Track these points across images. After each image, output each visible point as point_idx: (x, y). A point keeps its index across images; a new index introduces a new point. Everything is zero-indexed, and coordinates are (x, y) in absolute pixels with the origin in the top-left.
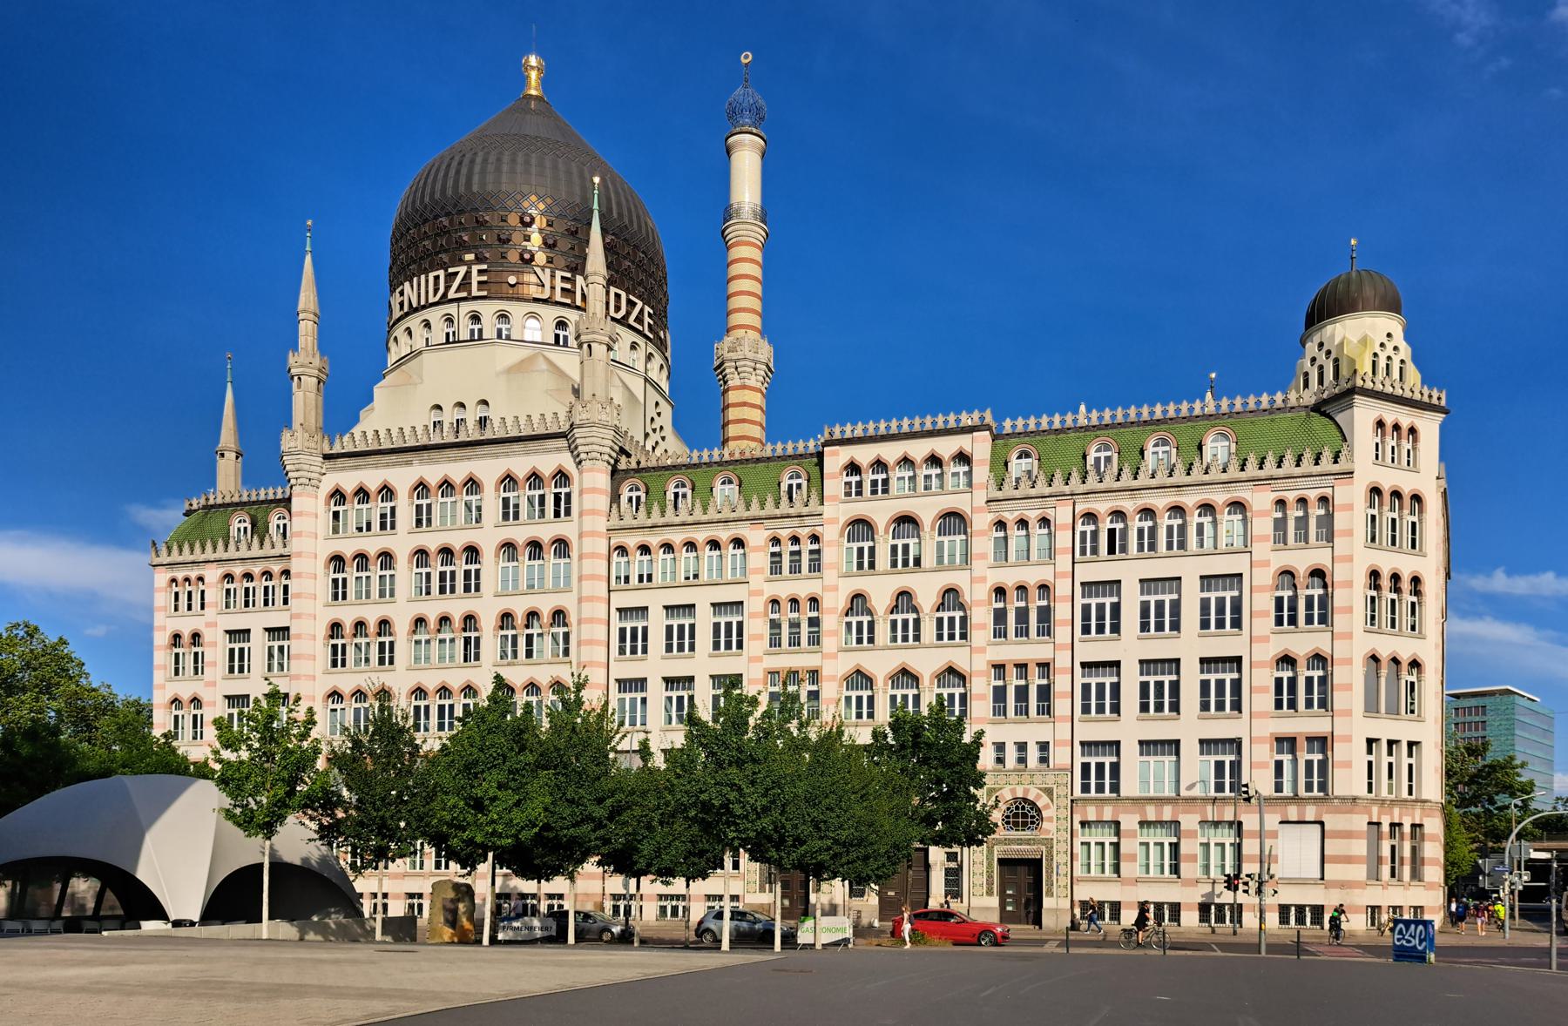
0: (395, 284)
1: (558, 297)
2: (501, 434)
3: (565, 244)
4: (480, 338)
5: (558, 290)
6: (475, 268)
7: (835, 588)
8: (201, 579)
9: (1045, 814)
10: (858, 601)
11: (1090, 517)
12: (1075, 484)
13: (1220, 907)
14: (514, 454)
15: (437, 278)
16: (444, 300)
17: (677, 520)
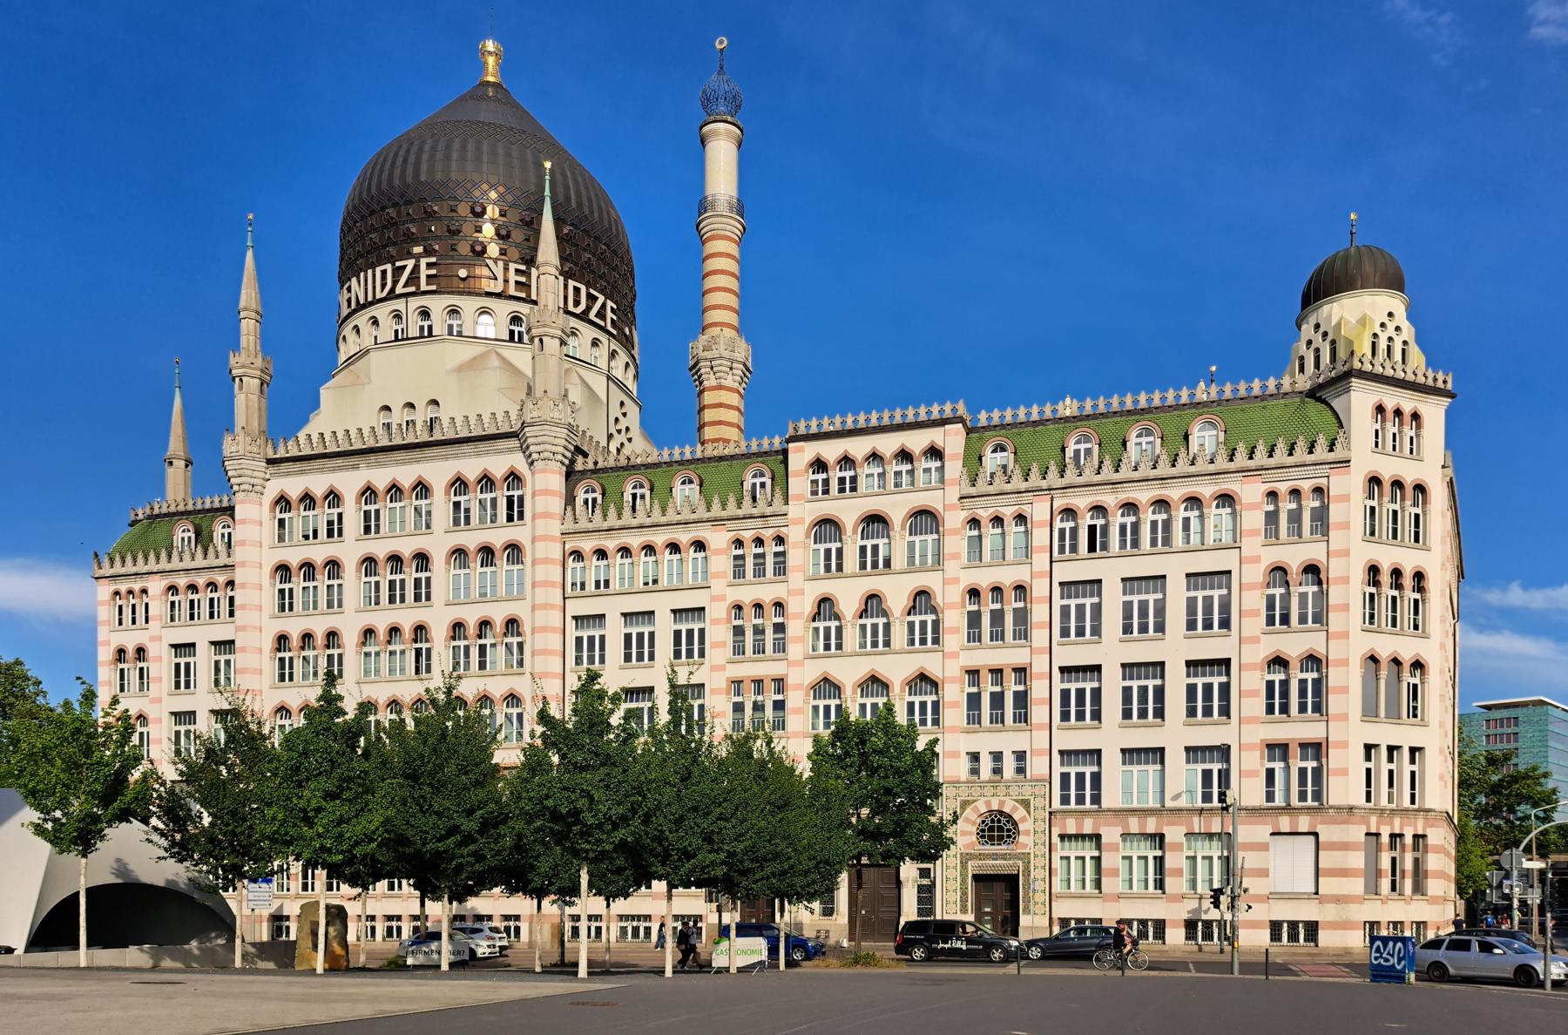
0: (343, 279)
1: (512, 291)
2: (450, 435)
3: (518, 235)
4: (430, 334)
5: (512, 284)
6: (423, 262)
7: (801, 592)
8: (144, 591)
9: (1021, 827)
10: (825, 606)
11: (1069, 512)
12: (1053, 478)
13: (1208, 924)
14: (465, 455)
15: (384, 272)
17: (635, 522)
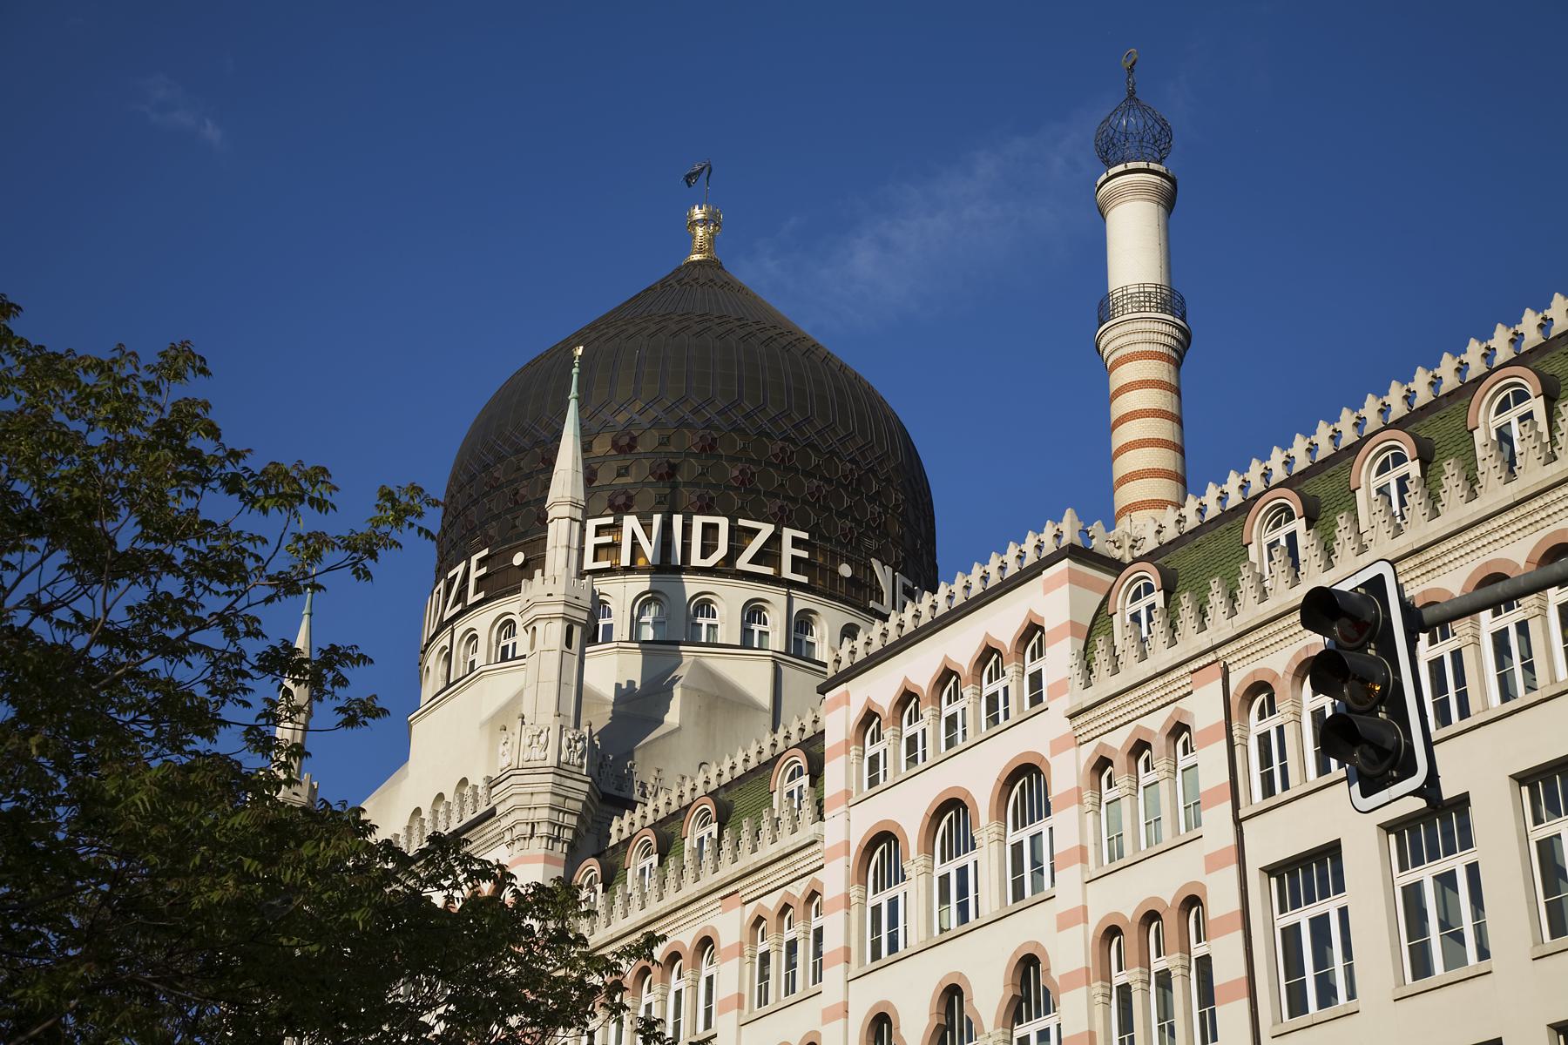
6: (788, 534)
15: (710, 530)
16: (725, 570)
